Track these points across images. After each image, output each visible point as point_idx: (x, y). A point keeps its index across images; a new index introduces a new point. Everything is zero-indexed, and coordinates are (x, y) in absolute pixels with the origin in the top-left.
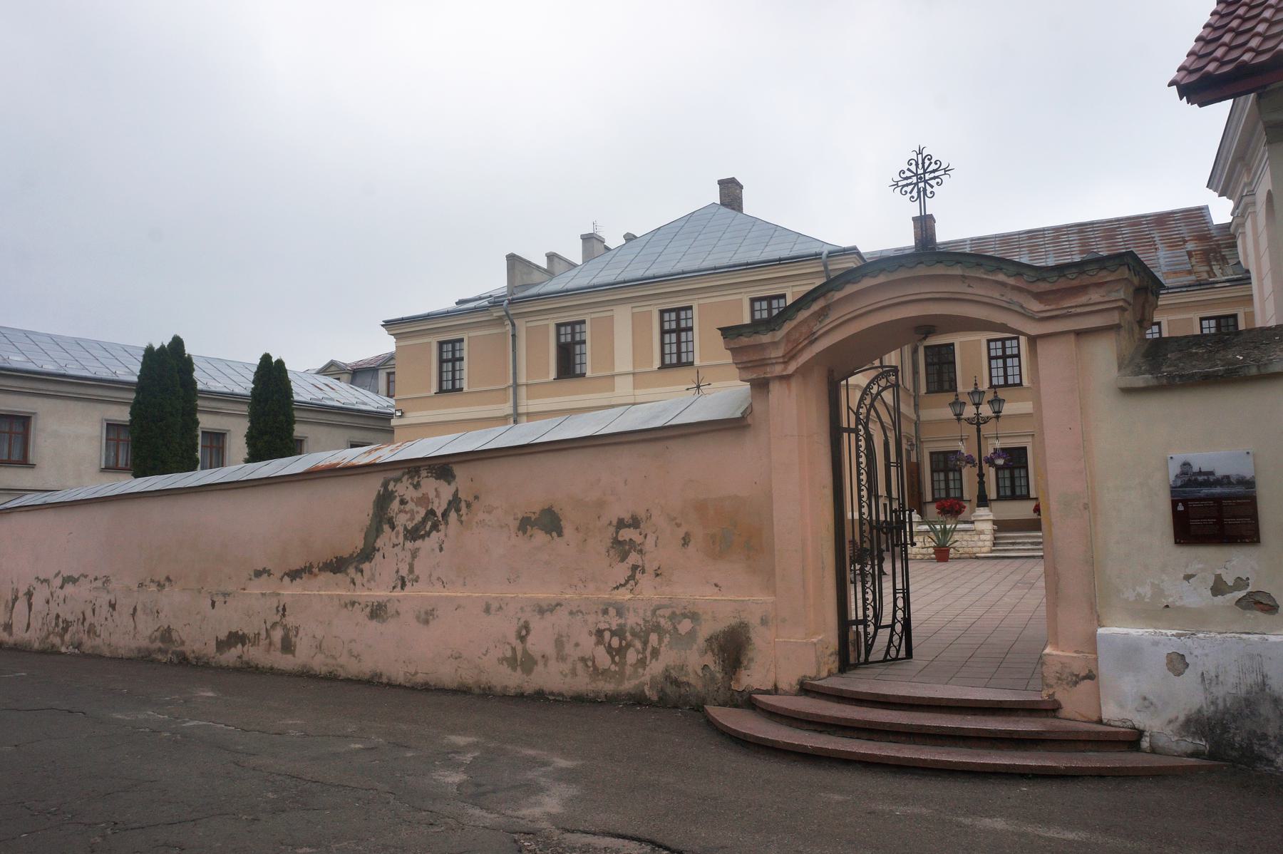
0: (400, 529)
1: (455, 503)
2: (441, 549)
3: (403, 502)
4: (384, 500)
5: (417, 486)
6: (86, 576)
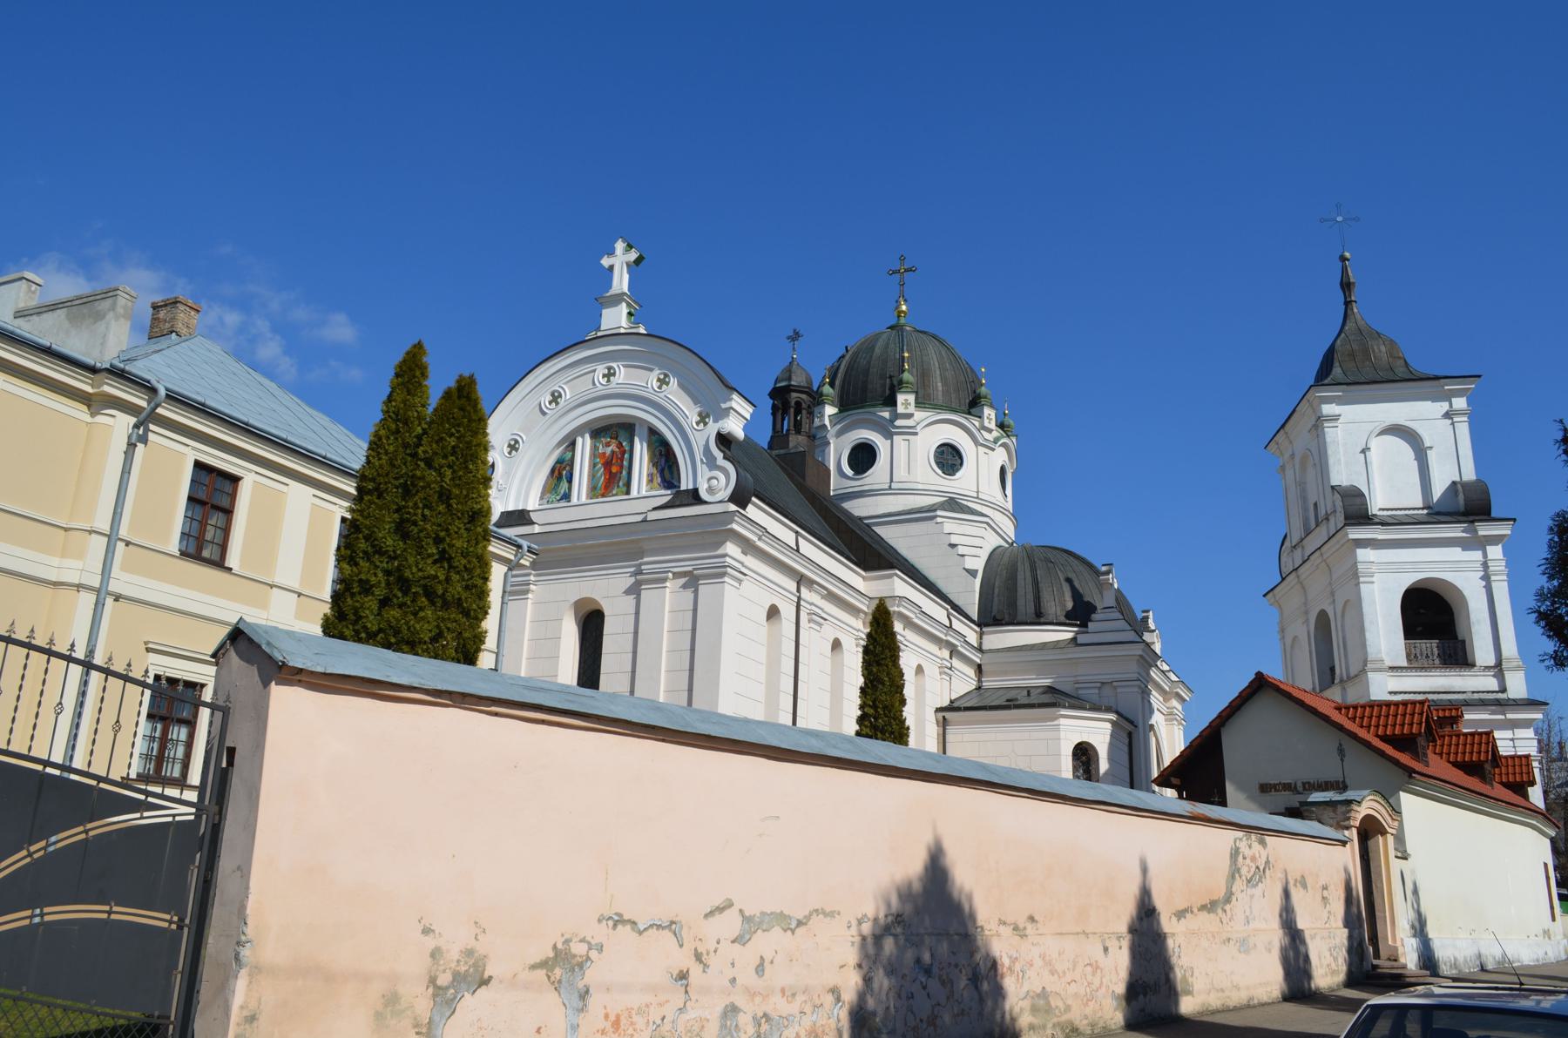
0: (1244, 878)
1: (1267, 862)
2: (1264, 896)
3: (1244, 858)
4: (1235, 853)
5: (1250, 847)
6: (830, 914)
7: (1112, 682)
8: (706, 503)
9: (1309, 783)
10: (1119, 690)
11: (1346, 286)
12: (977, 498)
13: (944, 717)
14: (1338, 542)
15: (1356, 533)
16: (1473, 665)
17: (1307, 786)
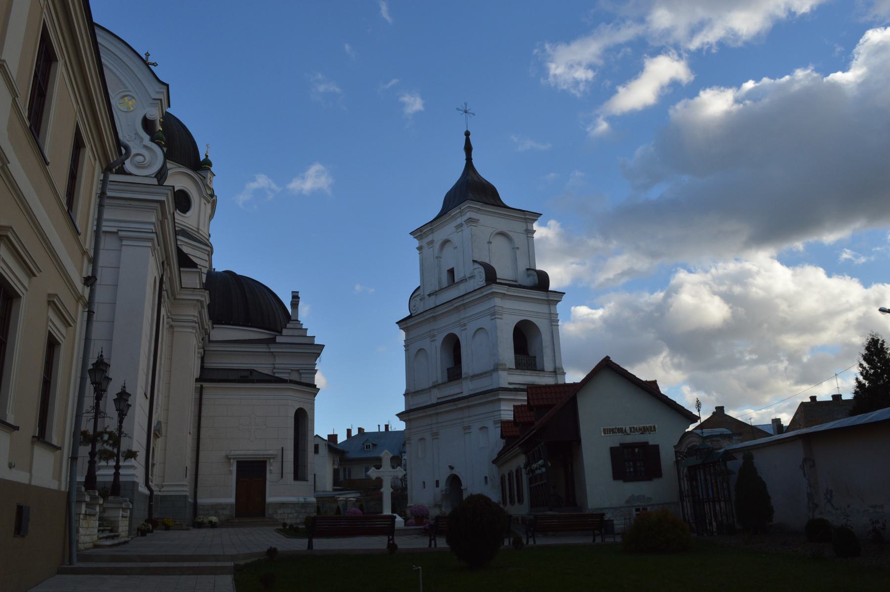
7: (298, 370)
8: (130, 174)
9: (634, 428)
10: (302, 376)
11: (468, 148)
12: (198, 232)
13: (202, 386)
14: (482, 293)
15: (496, 288)
16: (543, 370)
17: (632, 430)
